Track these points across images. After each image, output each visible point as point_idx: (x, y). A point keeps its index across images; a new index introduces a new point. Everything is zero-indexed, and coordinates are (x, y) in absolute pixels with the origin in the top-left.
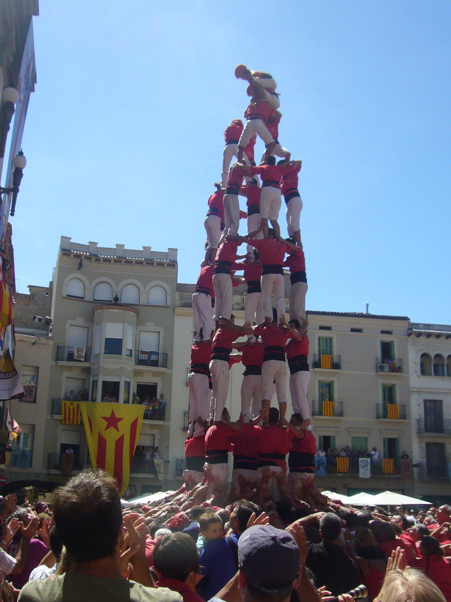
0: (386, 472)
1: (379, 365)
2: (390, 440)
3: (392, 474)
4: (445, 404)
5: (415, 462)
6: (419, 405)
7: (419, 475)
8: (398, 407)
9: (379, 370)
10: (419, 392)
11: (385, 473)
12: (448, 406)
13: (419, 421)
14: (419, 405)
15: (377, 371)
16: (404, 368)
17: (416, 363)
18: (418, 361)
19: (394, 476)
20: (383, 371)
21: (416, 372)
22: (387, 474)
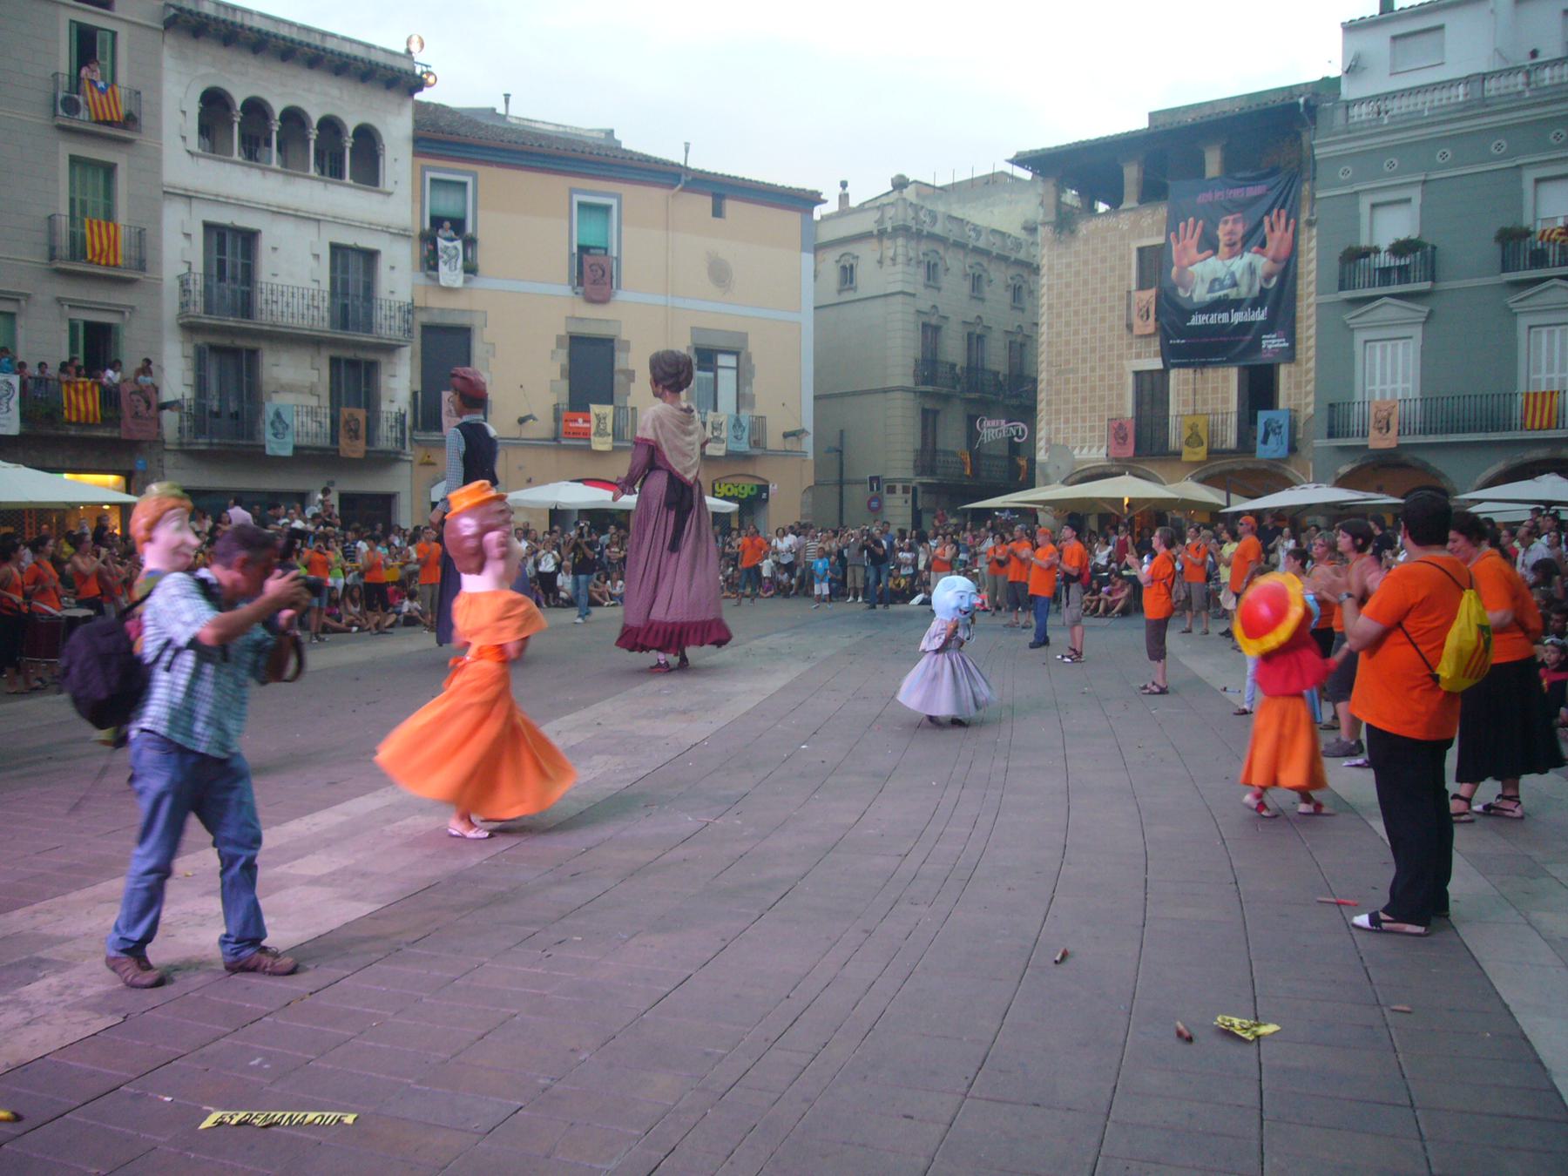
0: (74, 419)
1: (61, 95)
2: (90, 327)
3: (95, 426)
4: (265, 243)
5: (167, 395)
6: (187, 236)
7: (180, 432)
8: (122, 232)
9: (60, 111)
10: (190, 197)
11: (70, 422)
12: (275, 249)
13: (184, 282)
14: (187, 236)
15: (55, 114)
16: (145, 121)
17: (184, 112)
18: (194, 108)
19: (101, 433)
20: (76, 117)
21: (184, 138)
22: (78, 423)
